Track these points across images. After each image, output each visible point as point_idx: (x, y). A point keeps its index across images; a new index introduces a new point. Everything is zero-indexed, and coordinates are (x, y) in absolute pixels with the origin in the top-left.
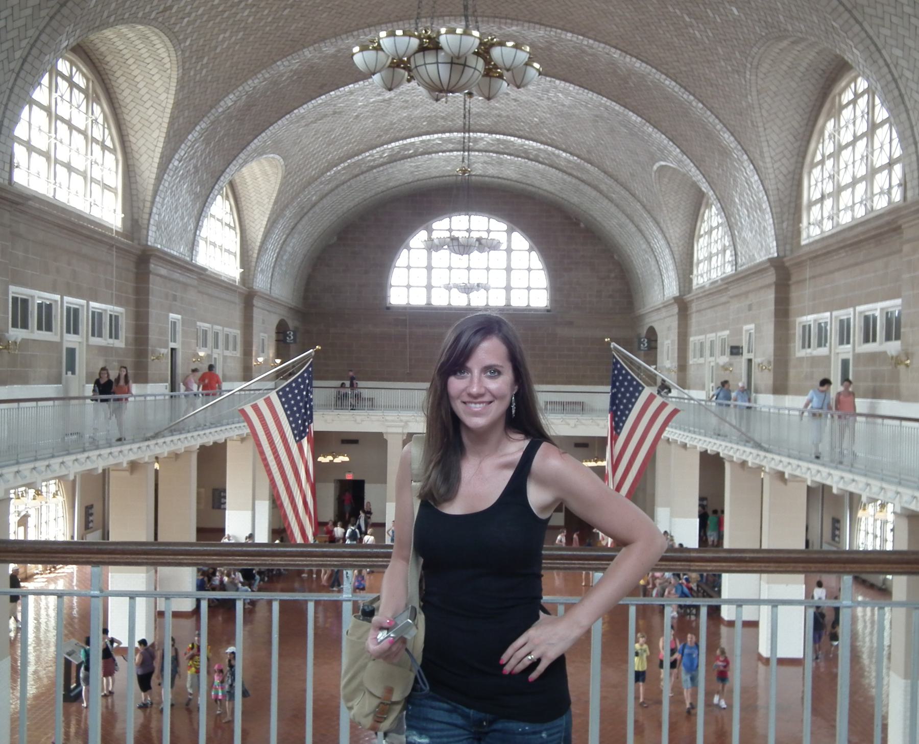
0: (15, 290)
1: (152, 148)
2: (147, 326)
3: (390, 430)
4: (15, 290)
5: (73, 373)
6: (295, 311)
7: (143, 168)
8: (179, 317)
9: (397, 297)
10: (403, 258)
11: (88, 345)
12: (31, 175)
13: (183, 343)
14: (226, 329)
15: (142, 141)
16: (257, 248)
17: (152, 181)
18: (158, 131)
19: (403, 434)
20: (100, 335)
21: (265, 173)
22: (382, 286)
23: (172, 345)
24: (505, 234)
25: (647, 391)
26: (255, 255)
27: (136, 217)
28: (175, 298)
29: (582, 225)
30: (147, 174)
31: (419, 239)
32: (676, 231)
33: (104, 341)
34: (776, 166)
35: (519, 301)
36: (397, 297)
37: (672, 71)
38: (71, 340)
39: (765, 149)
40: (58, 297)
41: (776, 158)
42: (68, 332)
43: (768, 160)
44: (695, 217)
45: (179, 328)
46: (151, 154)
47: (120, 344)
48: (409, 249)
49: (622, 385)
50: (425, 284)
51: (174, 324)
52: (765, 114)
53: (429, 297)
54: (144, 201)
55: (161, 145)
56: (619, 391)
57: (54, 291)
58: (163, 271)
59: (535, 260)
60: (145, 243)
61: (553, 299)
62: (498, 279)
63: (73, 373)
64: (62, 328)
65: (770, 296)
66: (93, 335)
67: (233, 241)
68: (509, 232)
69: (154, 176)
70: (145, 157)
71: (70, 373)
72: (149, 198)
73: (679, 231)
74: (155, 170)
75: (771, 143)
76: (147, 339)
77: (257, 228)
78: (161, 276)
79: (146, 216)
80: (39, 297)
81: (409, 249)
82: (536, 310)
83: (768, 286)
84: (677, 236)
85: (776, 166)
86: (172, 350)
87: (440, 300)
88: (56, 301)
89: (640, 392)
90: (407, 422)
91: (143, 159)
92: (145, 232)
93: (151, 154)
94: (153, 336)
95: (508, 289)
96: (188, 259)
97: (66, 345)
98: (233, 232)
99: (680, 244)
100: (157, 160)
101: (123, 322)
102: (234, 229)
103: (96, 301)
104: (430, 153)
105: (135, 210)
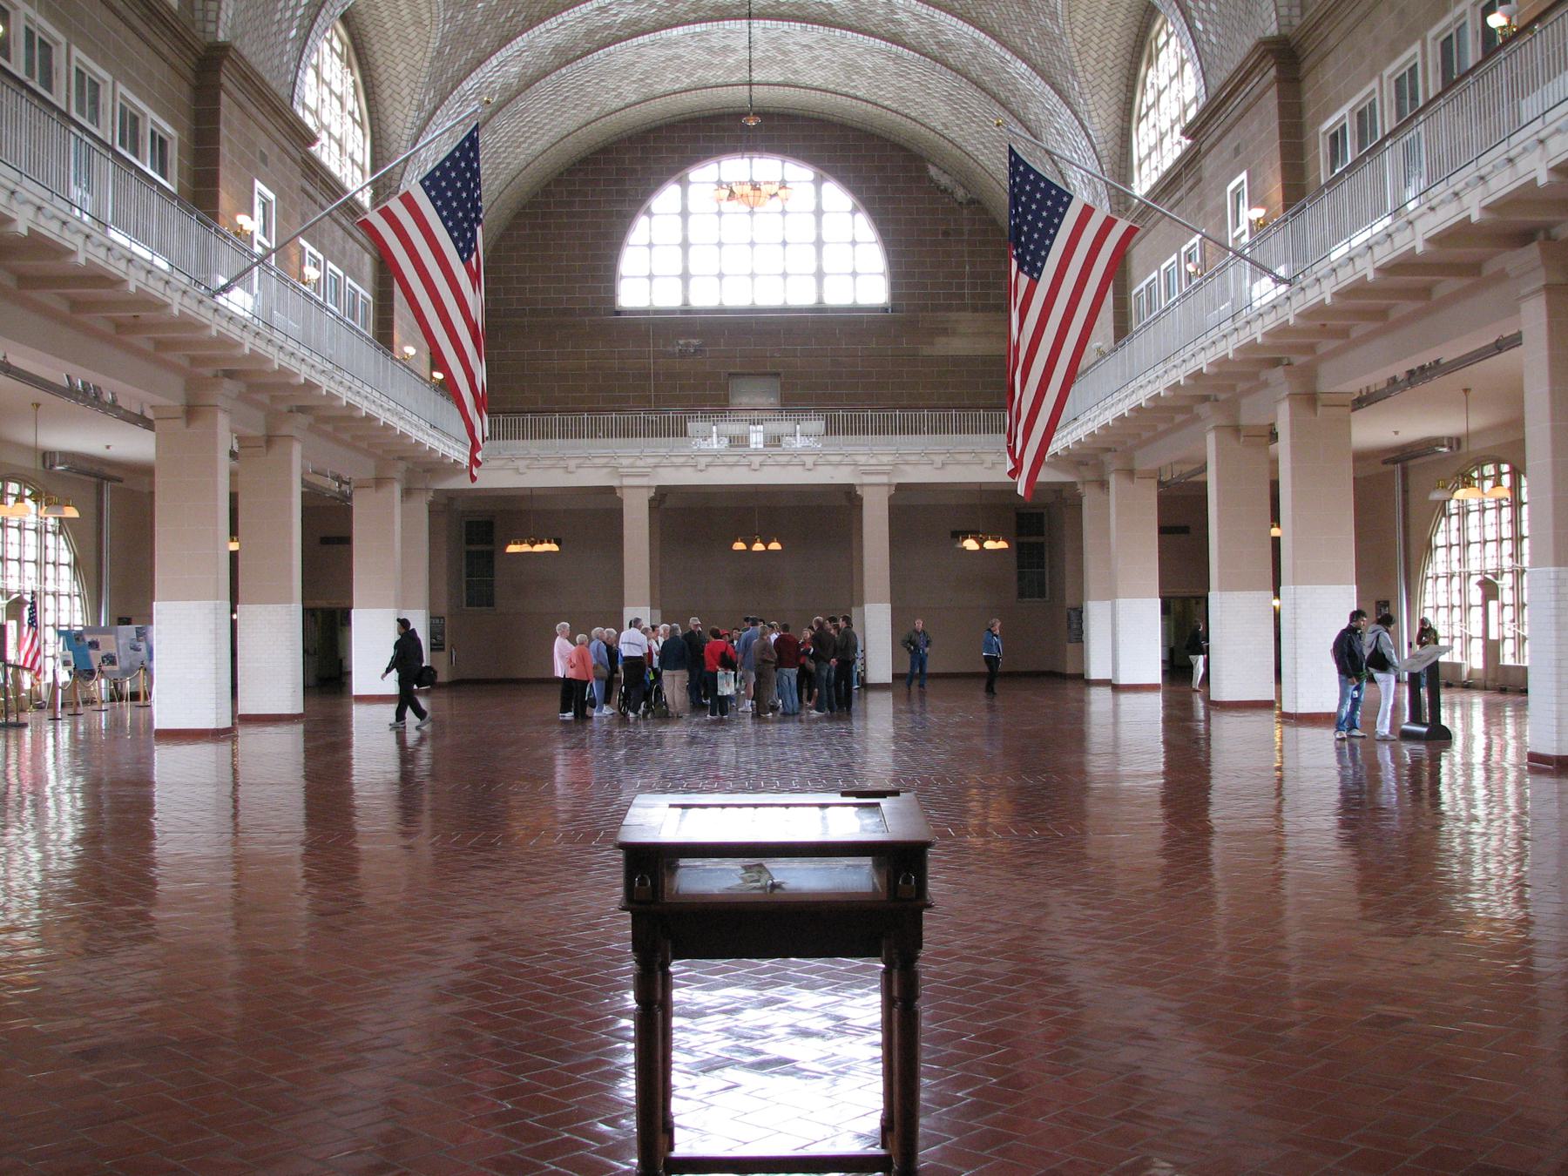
3: (627, 482)
10: (640, 231)
24: (812, 187)
28: (264, 159)
31: (666, 199)
35: (839, 295)
44: (1130, 83)
48: (649, 213)
59: (864, 228)
60: (210, 39)
61: (894, 296)
62: (804, 260)
65: (1271, 101)
68: (818, 182)
81: (649, 213)
87: (705, 297)
95: (820, 275)
98: (358, 131)
102: (361, 126)
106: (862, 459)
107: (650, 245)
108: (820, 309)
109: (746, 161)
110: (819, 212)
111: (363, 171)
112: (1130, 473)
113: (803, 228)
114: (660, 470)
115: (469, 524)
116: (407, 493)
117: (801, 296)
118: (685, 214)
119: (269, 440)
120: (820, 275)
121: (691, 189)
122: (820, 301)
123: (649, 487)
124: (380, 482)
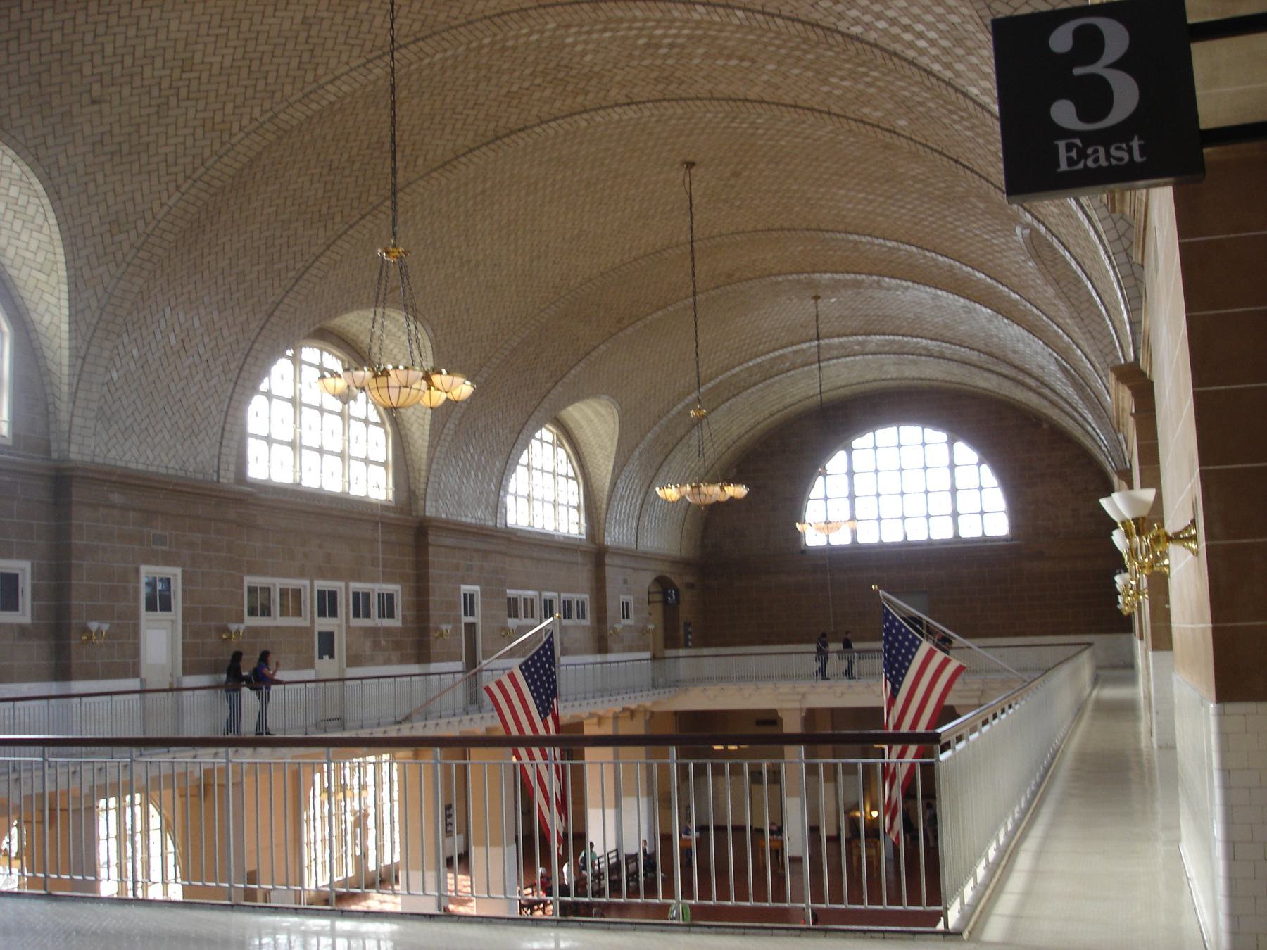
0: (249, 581)
2: (428, 601)
4: (249, 581)
5: (332, 656)
6: (682, 564)
7: (416, 437)
8: (477, 588)
9: (813, 537)
10: (818, 488)
11: (348, 628)
12: (266, 465)
13: (484, 617)
14: (563, 595)
16: (605, 497)
17: (426, 450)
19: (801, 709)
20: (367, 615)
21: (598, 414)
23: (469, 619)
24: (946, 447)
25: (925, 646)
26: (604, 506)
27: (413, 487)
29: (1045, 426)
30: (420, 442)
31: (837, 462)
33: (375, 621)
35: (970, 530)
38: (325, 624)
40: (307, 582)
42: (322, 613)
45: (478, 600)
47: (396, 623)
48: (825, 475)
49: (896, 639)
51: (470, 599)
54: (420, 470)
56: (892, 647)
57: (302, 575)
58: (449, 541)
59: (988, 476)
60: (421, 513)
61: (1014, 525)
62: (942, 504)
63: (332, 656)
64: (312, 613)
66: (356, 615)
67: (572, 492)
68: (951, 443)
69: (426, 444)
71: (326, 657)
72: (424, 467)
74: (427, 438)
75: (1095, 334)
76: (428, 616)
78: (446, 547)
79: (423, 486)
80: (277, 583)
86: (471, 627)
87: (868, 537)
88: (305, 586)
89: (917, 647)
90: (804, 695)
91: (414, 428)
92: (421, 502)
94: (434, 613)
95: (955, 515)
96: (491, 523)
97: (317, 629)
100: (427, 428)
101: (398, 601)
103: (359, 579)
105: (412, 481)
109: (895, 428)
110: (952, 466)
111: (578, 508)
113: (940, 479)
117: (942, 531)
118: (851, 473)
120: (955, 515)
122: (956, 535)
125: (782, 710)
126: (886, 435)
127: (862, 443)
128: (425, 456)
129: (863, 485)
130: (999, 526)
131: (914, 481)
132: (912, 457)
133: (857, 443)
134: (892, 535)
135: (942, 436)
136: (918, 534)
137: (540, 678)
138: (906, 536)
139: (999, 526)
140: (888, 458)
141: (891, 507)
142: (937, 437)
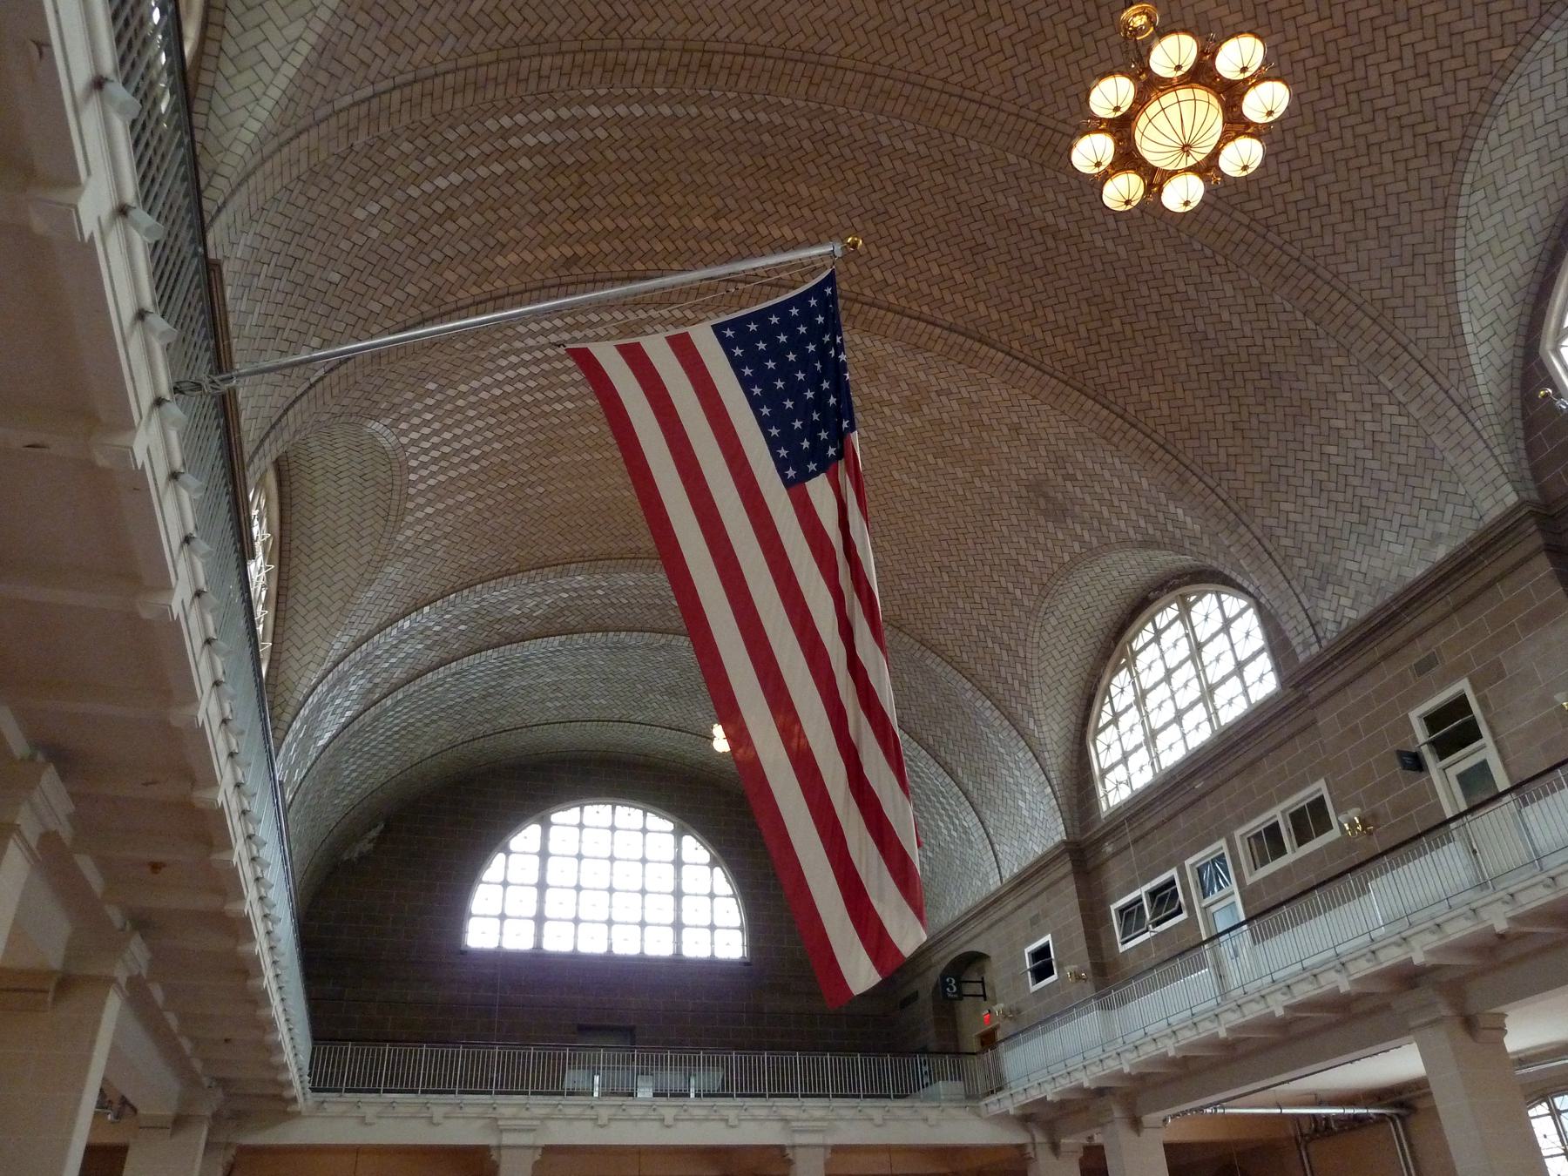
1: (274, 61)
3: (508, 1139)
7: (234, 102)
9: (480, 934)
10: (496, 868)
15: (255, 36)
17: (248, 137)
18: (301, 23)
22: (456, 912)
24: (671, 838)
31: (526, 838)
32: (1052, 730)
34: (1484, 349)
35: (696, 948)
36: (480, 934)
37: (1260, 215)
39: (1465, 317)
41: (1484, 335)
43: (1469, 338)
46: (267, 74)
48: (508, 852)
50: (533, 913)
52: (1472, 243)
53: (539, 935)
55: (298, 60)
59: (721, 881)
62: (661, 909)
68: (679, 833)
70: (247, 77)
73: (1056, 728)
75: (1474, 304)
77: (304, 662)
81: (508, 852)
82: (729, 964)
83: (1537, 552)
84: (1055, 738)
85: (1484, 349)
87: (558, 941)
93: (267, 74)
95: (678, 926)
99: (1059, 752)
100: (275, 93)
104: (606, 630)
106: (792, 1113)
107: (505, 884)
108: (677, 966)
109: (609, 807)
110: (678, 863)
112: (1136, 1124)
113: (662, 877)
114: (550, 1123)
115: (1292, 815)
116: (210, 1146)
117: (659, 946)
118: (544, 854)
119: (66, 984)
121: (553, 830)
122: (678, 953)
123: (535, 1147)
124: (180, 1122)
125: (499, 1147)
126: (597, 813)
127: (564, 817)
128: (240, 149)
129: (559, 871)
130: (732, 946)
131: (628, 876)
132: (629, 844)
133: (557, 817)
134: (592, 943)
135: (670, 826)
136: (627, 945)
137: (785, 371)
138: (610, 945)
139: (732, 946)
140: (596, 841)
141: (594, 906)
142: (661, 825)
